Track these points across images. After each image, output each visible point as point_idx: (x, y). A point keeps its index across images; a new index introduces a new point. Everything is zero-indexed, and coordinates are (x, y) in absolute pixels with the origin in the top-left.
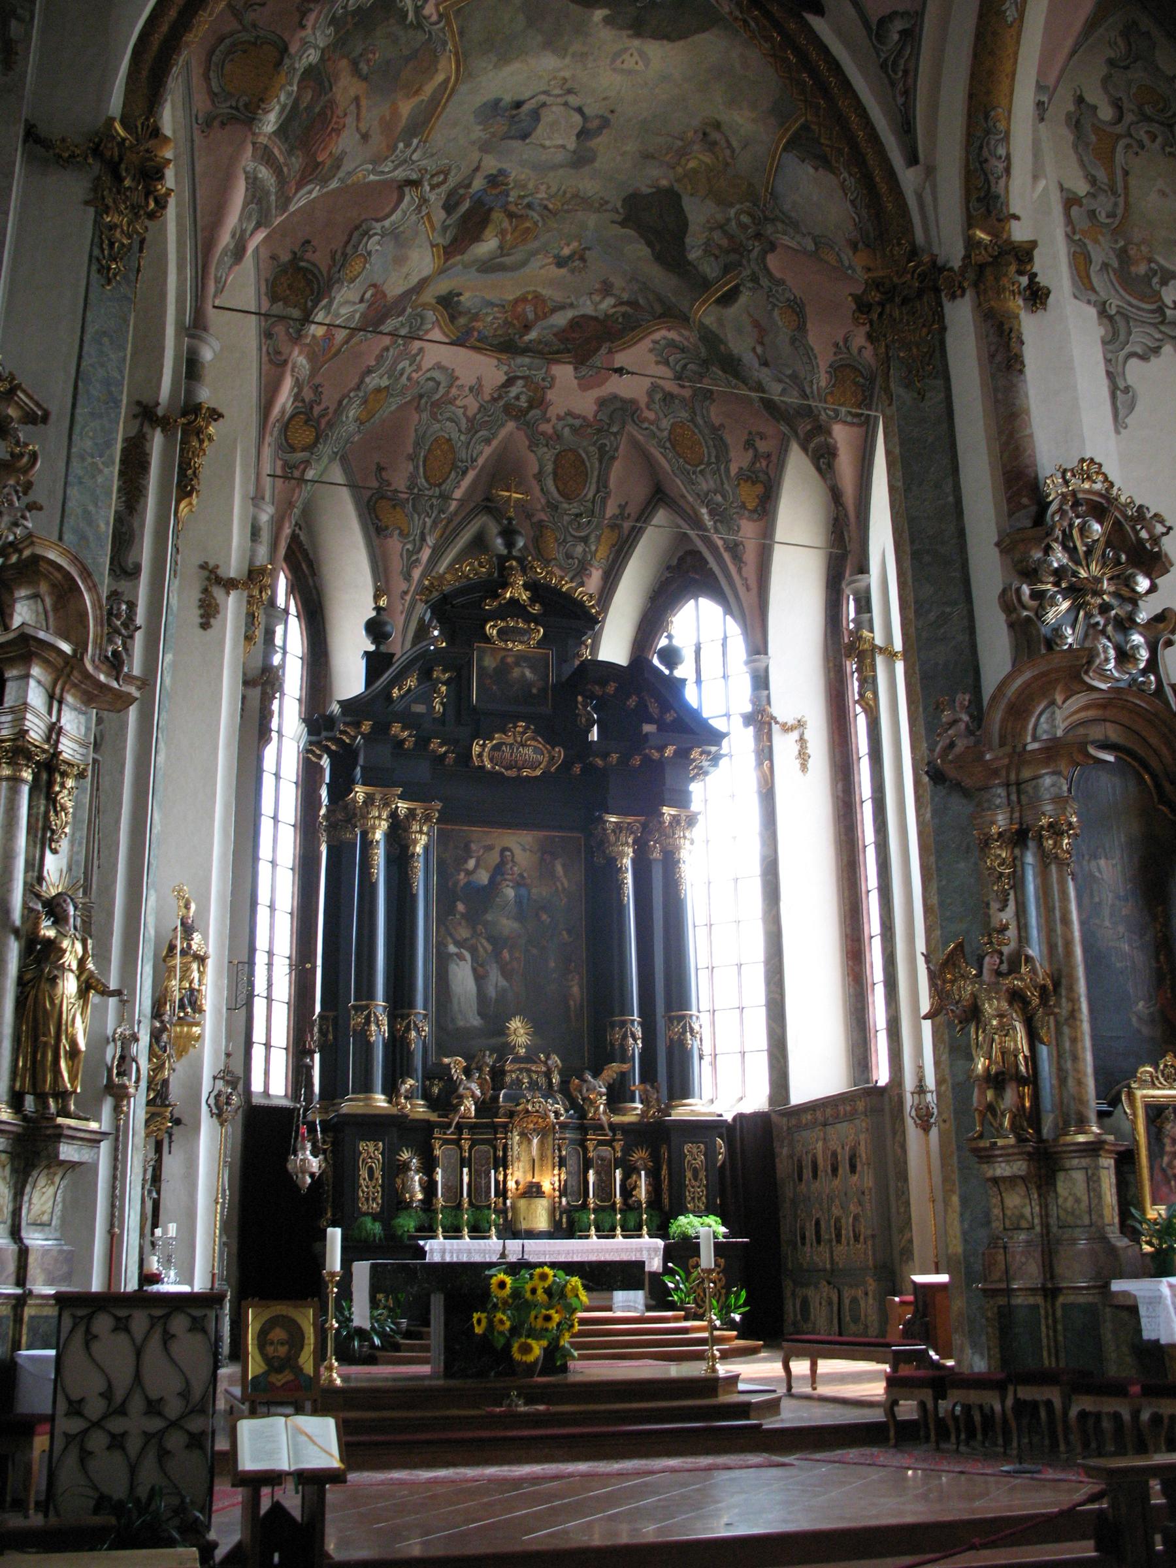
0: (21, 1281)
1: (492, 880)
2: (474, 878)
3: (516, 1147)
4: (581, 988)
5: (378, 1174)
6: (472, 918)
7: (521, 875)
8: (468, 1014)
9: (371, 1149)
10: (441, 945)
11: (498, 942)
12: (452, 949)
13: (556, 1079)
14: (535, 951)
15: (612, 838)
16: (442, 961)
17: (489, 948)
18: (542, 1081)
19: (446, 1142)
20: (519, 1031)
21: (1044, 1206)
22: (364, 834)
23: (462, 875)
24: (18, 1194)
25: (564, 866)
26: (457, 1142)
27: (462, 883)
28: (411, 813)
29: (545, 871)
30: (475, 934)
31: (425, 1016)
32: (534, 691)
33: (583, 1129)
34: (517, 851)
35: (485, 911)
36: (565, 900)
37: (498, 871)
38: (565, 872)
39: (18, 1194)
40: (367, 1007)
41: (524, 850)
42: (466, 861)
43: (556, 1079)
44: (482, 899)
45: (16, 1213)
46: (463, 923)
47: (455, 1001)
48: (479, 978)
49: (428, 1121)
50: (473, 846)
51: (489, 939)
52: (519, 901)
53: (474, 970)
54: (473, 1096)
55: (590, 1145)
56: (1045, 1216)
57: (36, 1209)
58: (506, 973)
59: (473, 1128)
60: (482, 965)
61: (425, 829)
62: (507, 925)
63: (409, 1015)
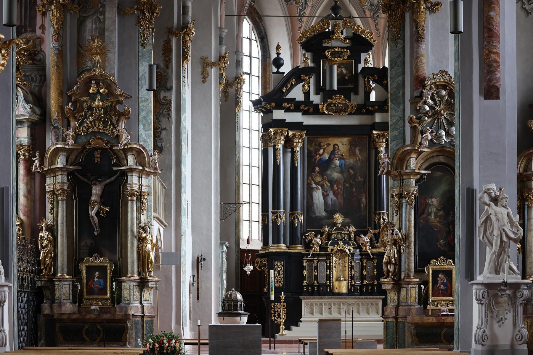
0: (143, 313)
1: (330, 157)
2: (322, 157)
3: (334, 262)
4: (366, 199)
5: (281, 273)
6: (322, 173)
7: (342, 155)
8: (320, 211)
9: (279, 264)
10: (309, 184)
11: (332, 182)
12: (314, 186)
13: (353, 235)
14: (347, 185)
15: (377, 140)
16: (311, 190)
17: (329, 184)
18: (346, 237)
19: (308, 260)
20: (339, 218)
21: (399, 297)
22: (275, 146)
23: (318, 156)
24: (141, 294)
25: (359, 150)
26: (312, 260)
27: (318, 159)
28: (294, 135)
29: (351, 152)
30: (323, 179)
31: (301, 214)
32: (346, 78)
33: (361, 254)
34: (340, 145)
35: (327, 170)
36: (360, 164)
37: (333, 153)
38: (360, 153)
39: (141, 294)
40: (277, 212)
41: (343, 144)
42: (319, 151)
43: (353, 235)
44: (327, 165)
45: (141, 298)
46: (318, 175)
47: (315, 206)
48: (325, 197)
49: (300, 253)
50: (322, 144)
51: (329, 181)
52: (341, 166)
53: (323, 193)
54: (318, 244)
55: (364, 261)
56: (399, 299)
57: (145, 297)
58: (335, 194)
59: (318, 255)
60: (326, 192)
61: (300, 141)
62: (336, 175)
63: (295, 213)
